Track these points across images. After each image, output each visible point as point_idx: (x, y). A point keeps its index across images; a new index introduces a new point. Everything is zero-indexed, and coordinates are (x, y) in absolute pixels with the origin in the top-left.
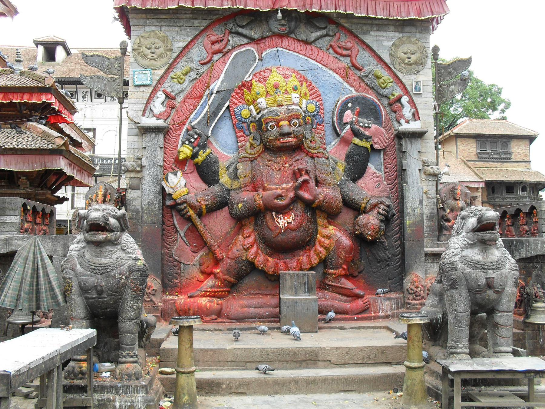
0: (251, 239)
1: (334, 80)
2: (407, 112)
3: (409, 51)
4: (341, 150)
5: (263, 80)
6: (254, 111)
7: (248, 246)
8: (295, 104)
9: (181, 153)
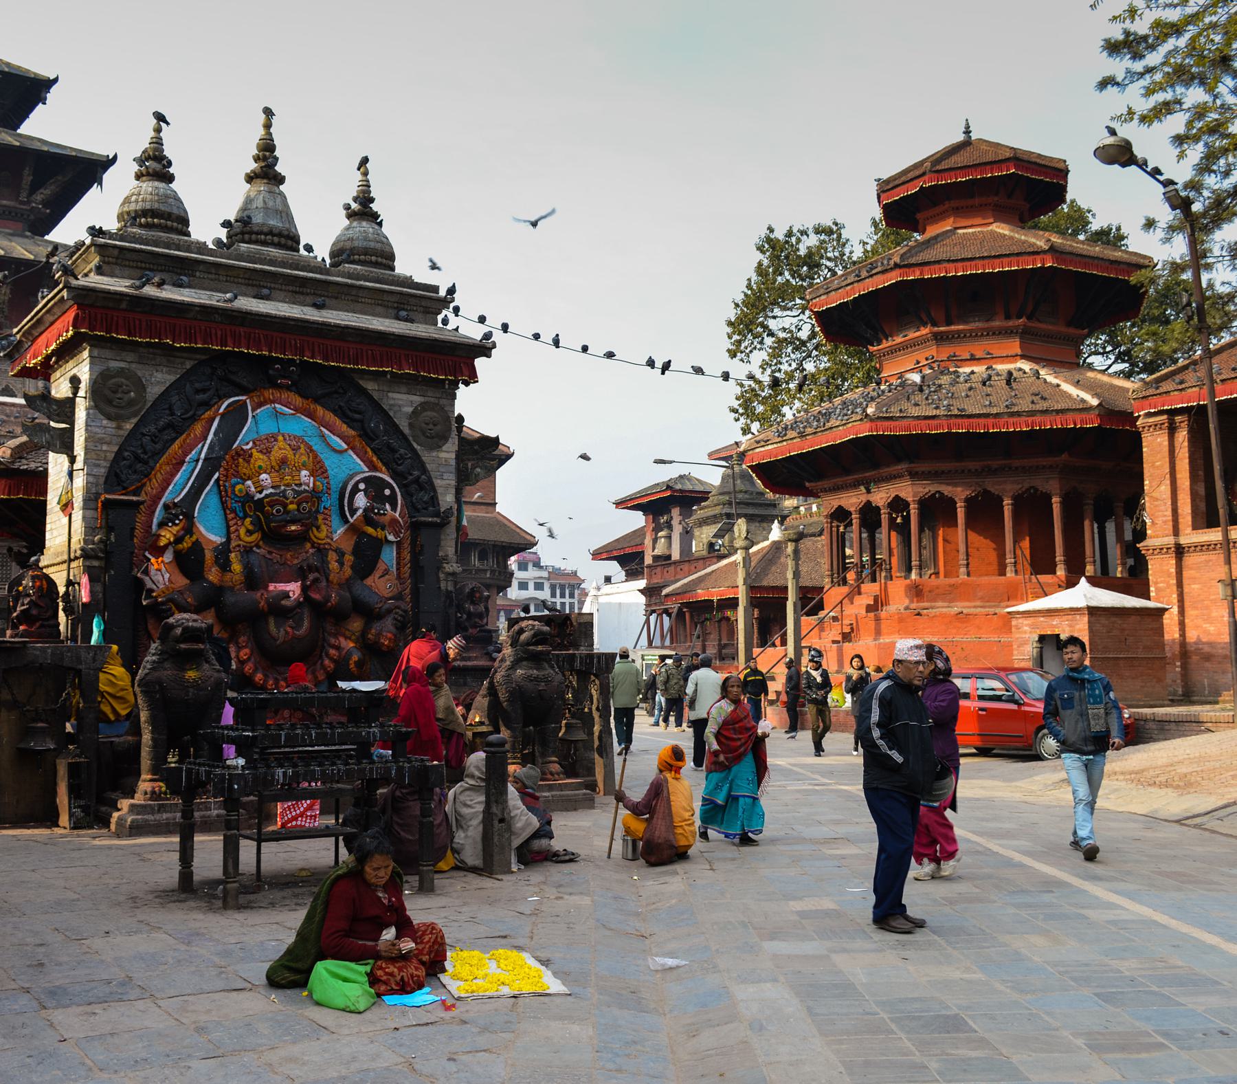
0: (247, 651)
5: (267, 452)
6: (253, 489)
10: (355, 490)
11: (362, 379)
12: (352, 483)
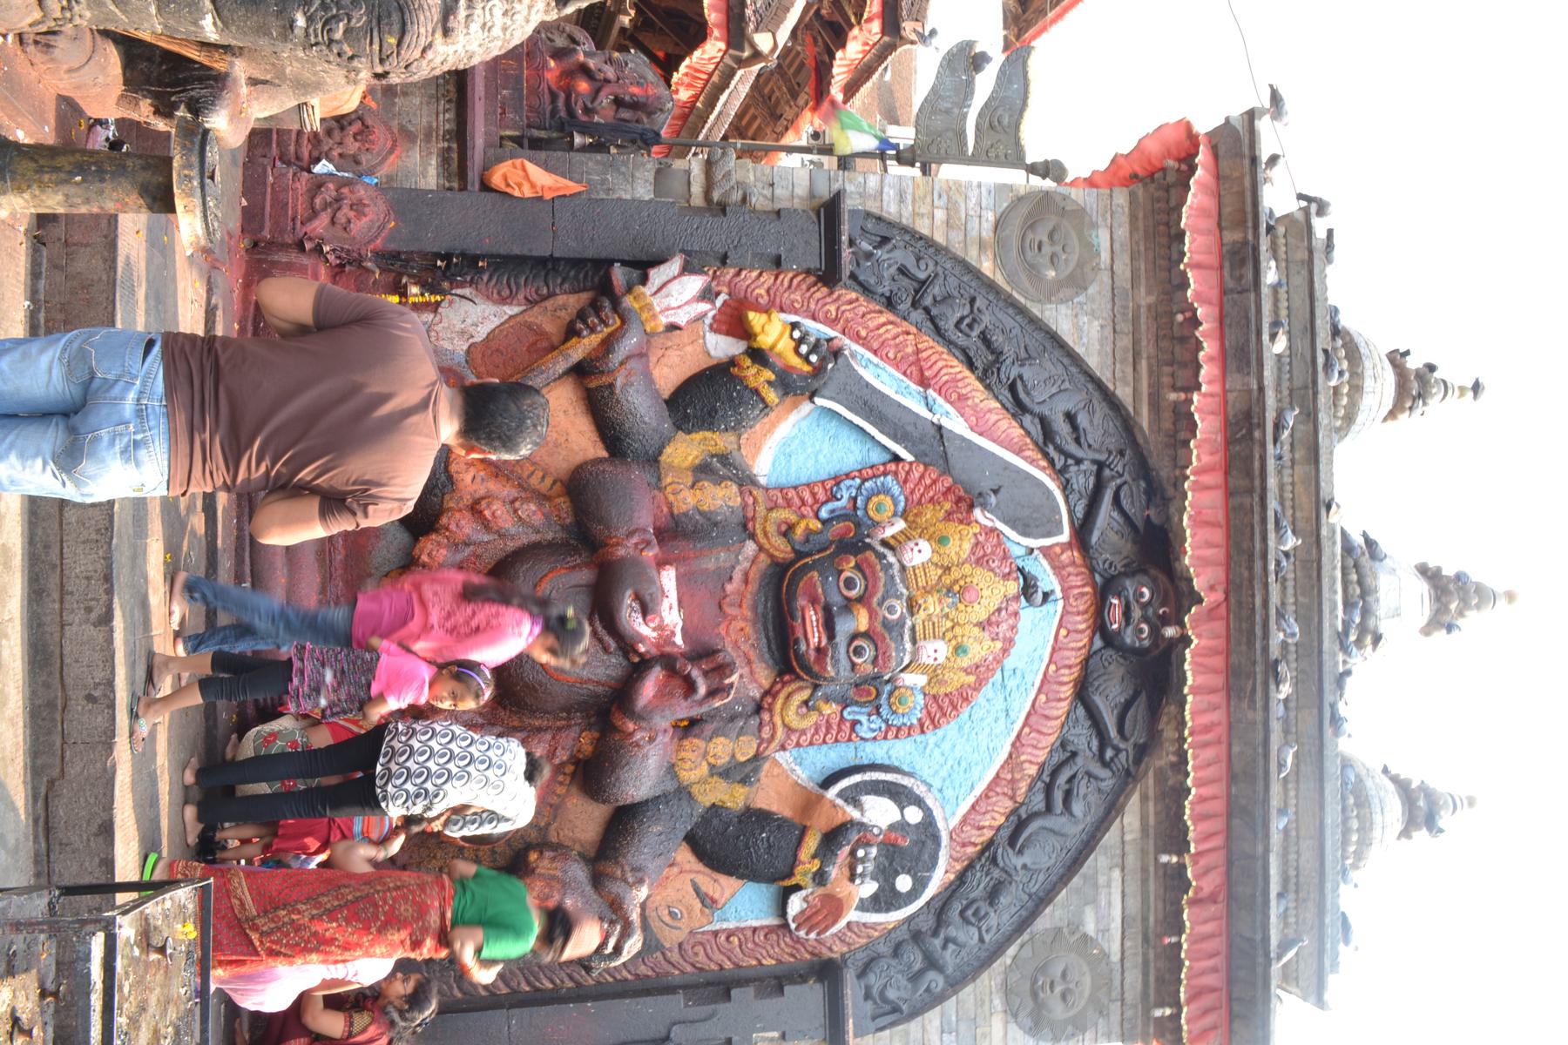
1: (980, 767)
3: (1072, 986)
4: (779, 794)
6: (889, 532)
7: (487, 513)
8: (915, 653)
9: (764, 317)
10: (900, 795)
11: (1144, 798)
12: (920, 790)
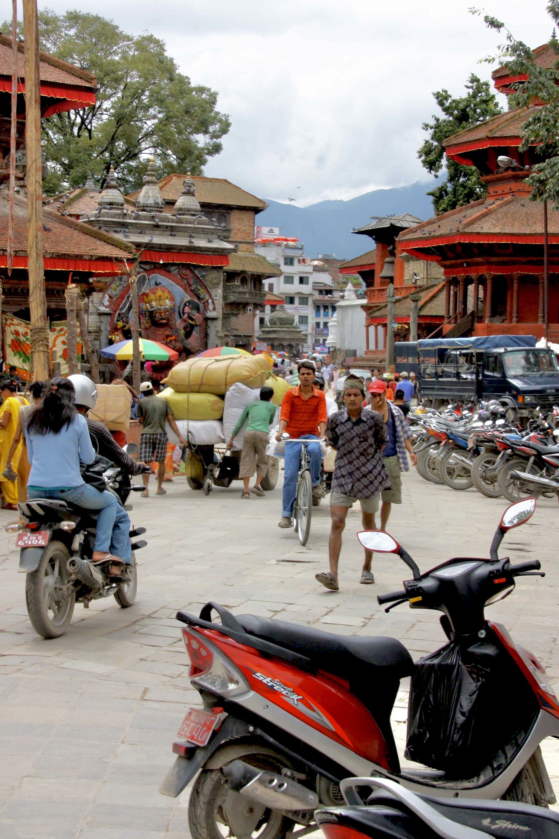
2: (211, 307)
5: (154, 293)
